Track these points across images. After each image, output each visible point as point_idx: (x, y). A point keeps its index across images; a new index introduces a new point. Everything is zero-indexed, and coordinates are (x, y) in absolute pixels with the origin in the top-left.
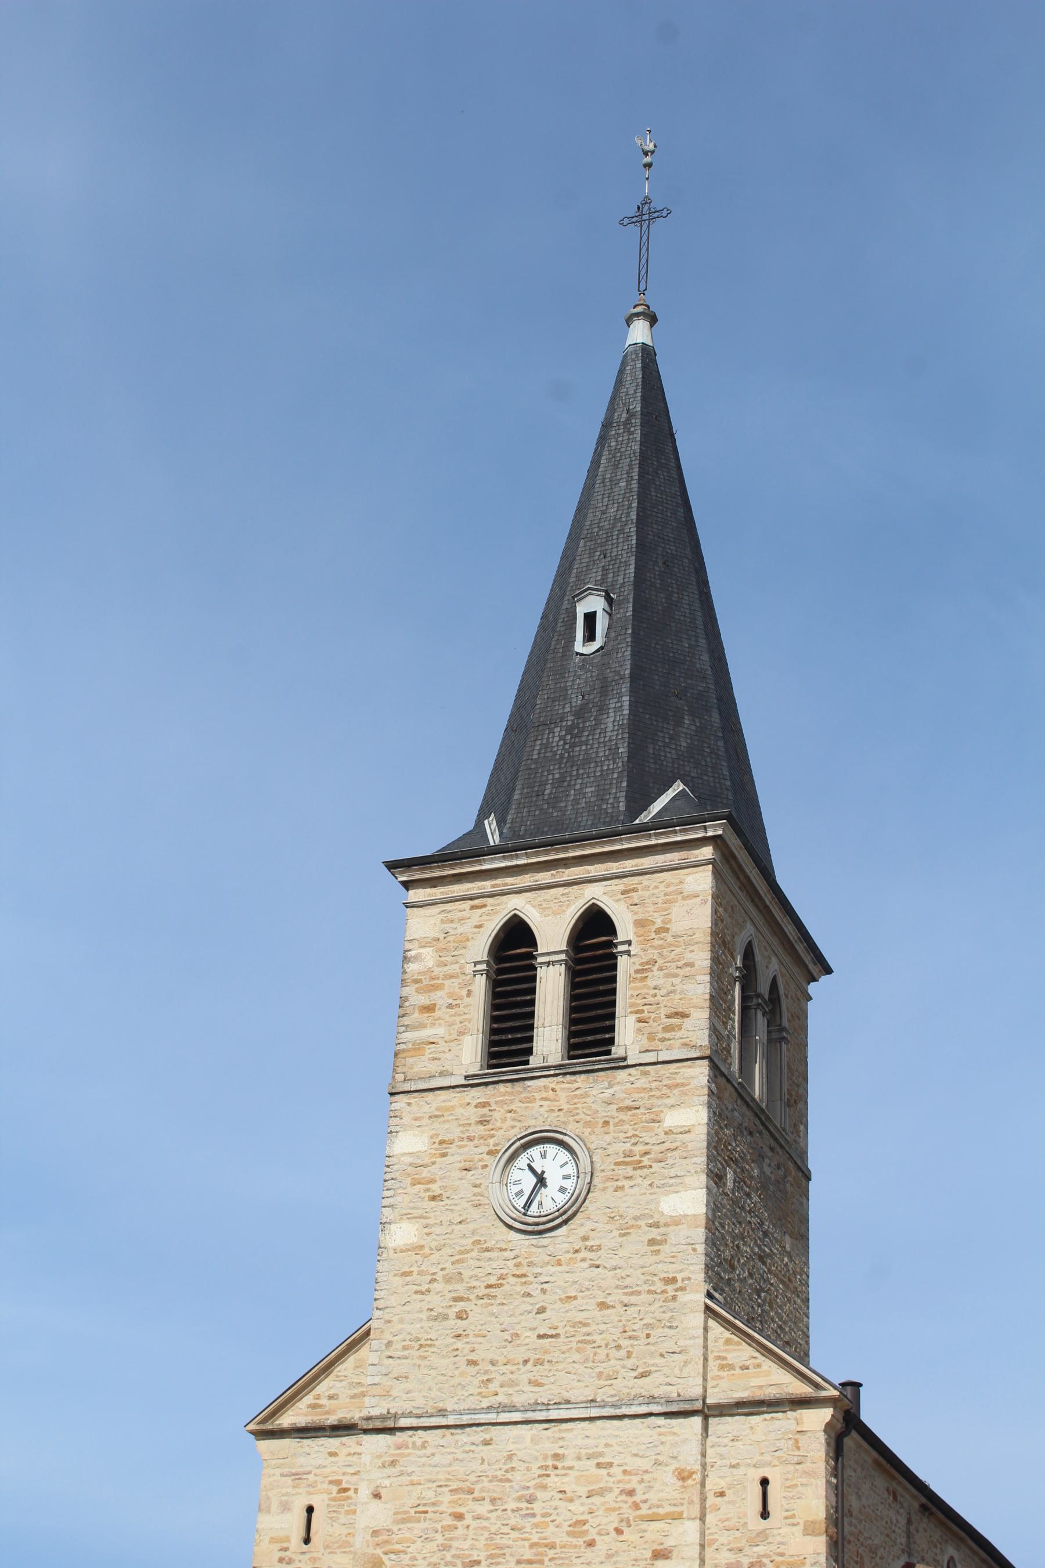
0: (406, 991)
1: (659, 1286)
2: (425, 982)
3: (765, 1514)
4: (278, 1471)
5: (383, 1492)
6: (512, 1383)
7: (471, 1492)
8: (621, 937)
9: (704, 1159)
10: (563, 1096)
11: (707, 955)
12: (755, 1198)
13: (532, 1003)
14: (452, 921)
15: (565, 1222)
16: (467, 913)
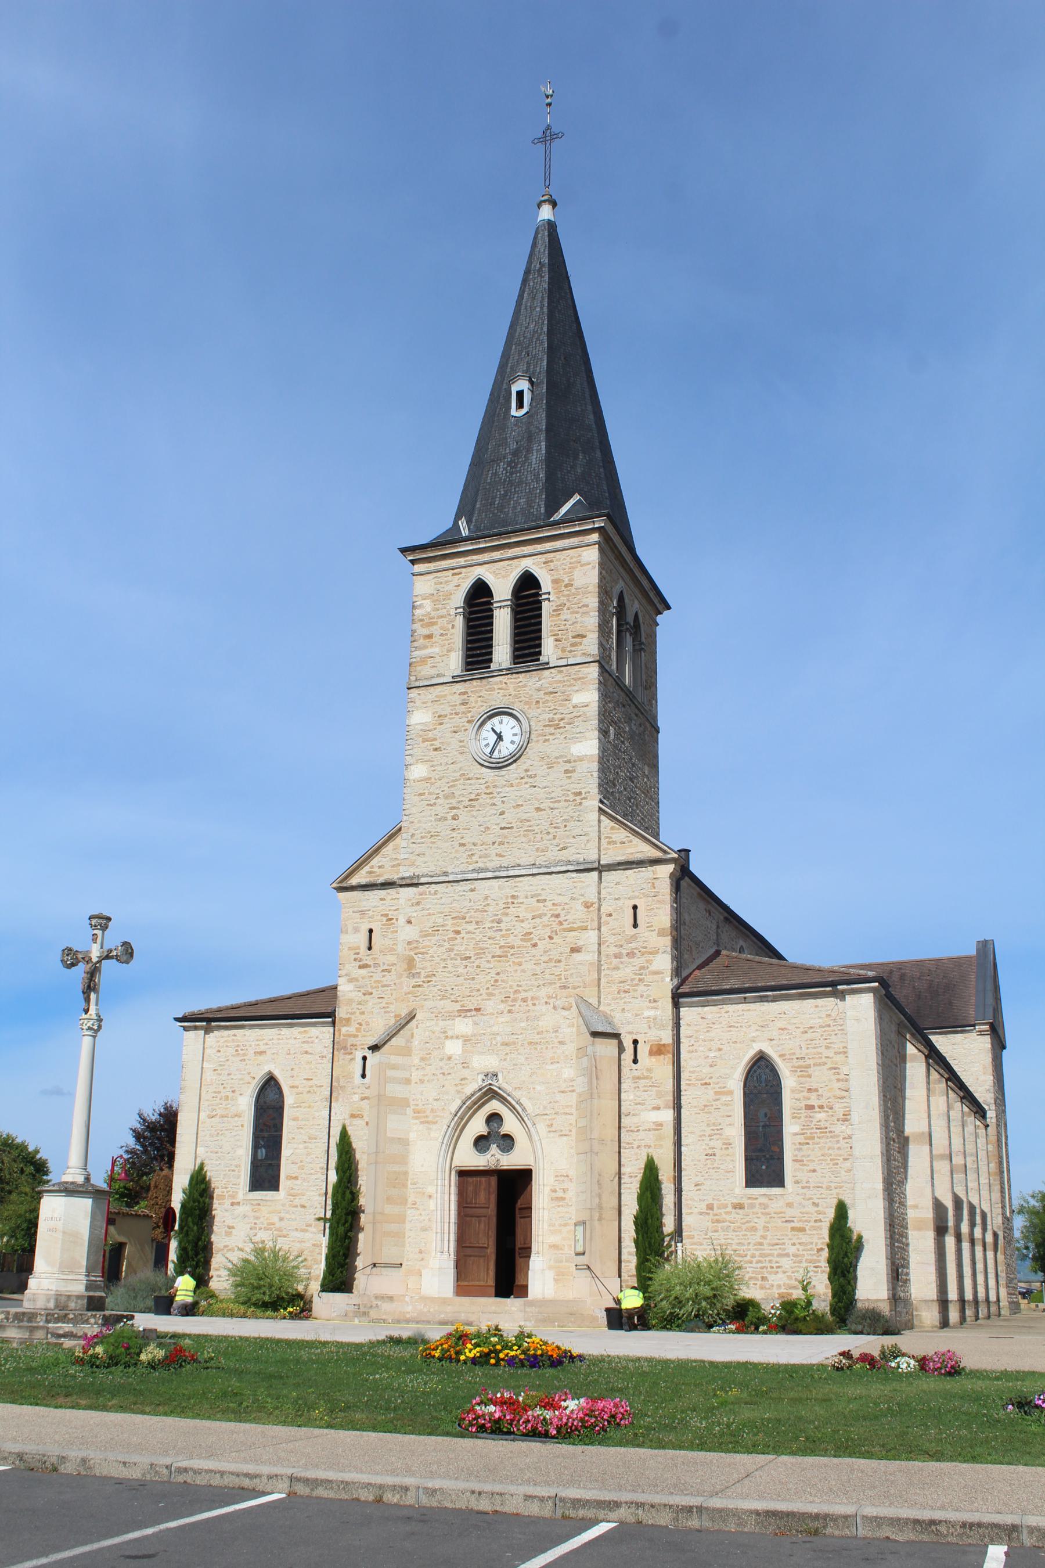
0: (415, 626)
1: (571, 797)
3: (635, 926)
4: (351, 910)
5: (413, 920)
6: (486, 856)
8: (544, 590)
9: (597, 722)
10: (511, 686)
11: (597, 600)
12: (627, 744)
13: (491, 631)
14: (441, 583)
15: (515, 761)
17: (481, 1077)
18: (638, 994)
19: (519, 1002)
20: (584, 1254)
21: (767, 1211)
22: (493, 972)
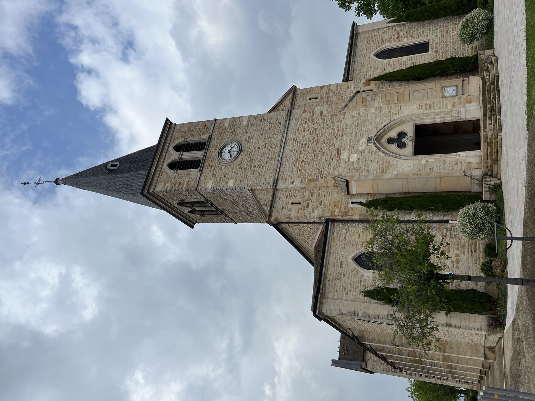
1: (261, 123)
2: (173, 185)
4: (281, 213)
5: (292, 181)
6: (274, 152)
7: (297, 159)
16: (162, 177)
17: (369, 144)
18: (344, 93)
19: (339, 133)
20: (457, 86)
21: (438, 43)
22: (323, 145)
